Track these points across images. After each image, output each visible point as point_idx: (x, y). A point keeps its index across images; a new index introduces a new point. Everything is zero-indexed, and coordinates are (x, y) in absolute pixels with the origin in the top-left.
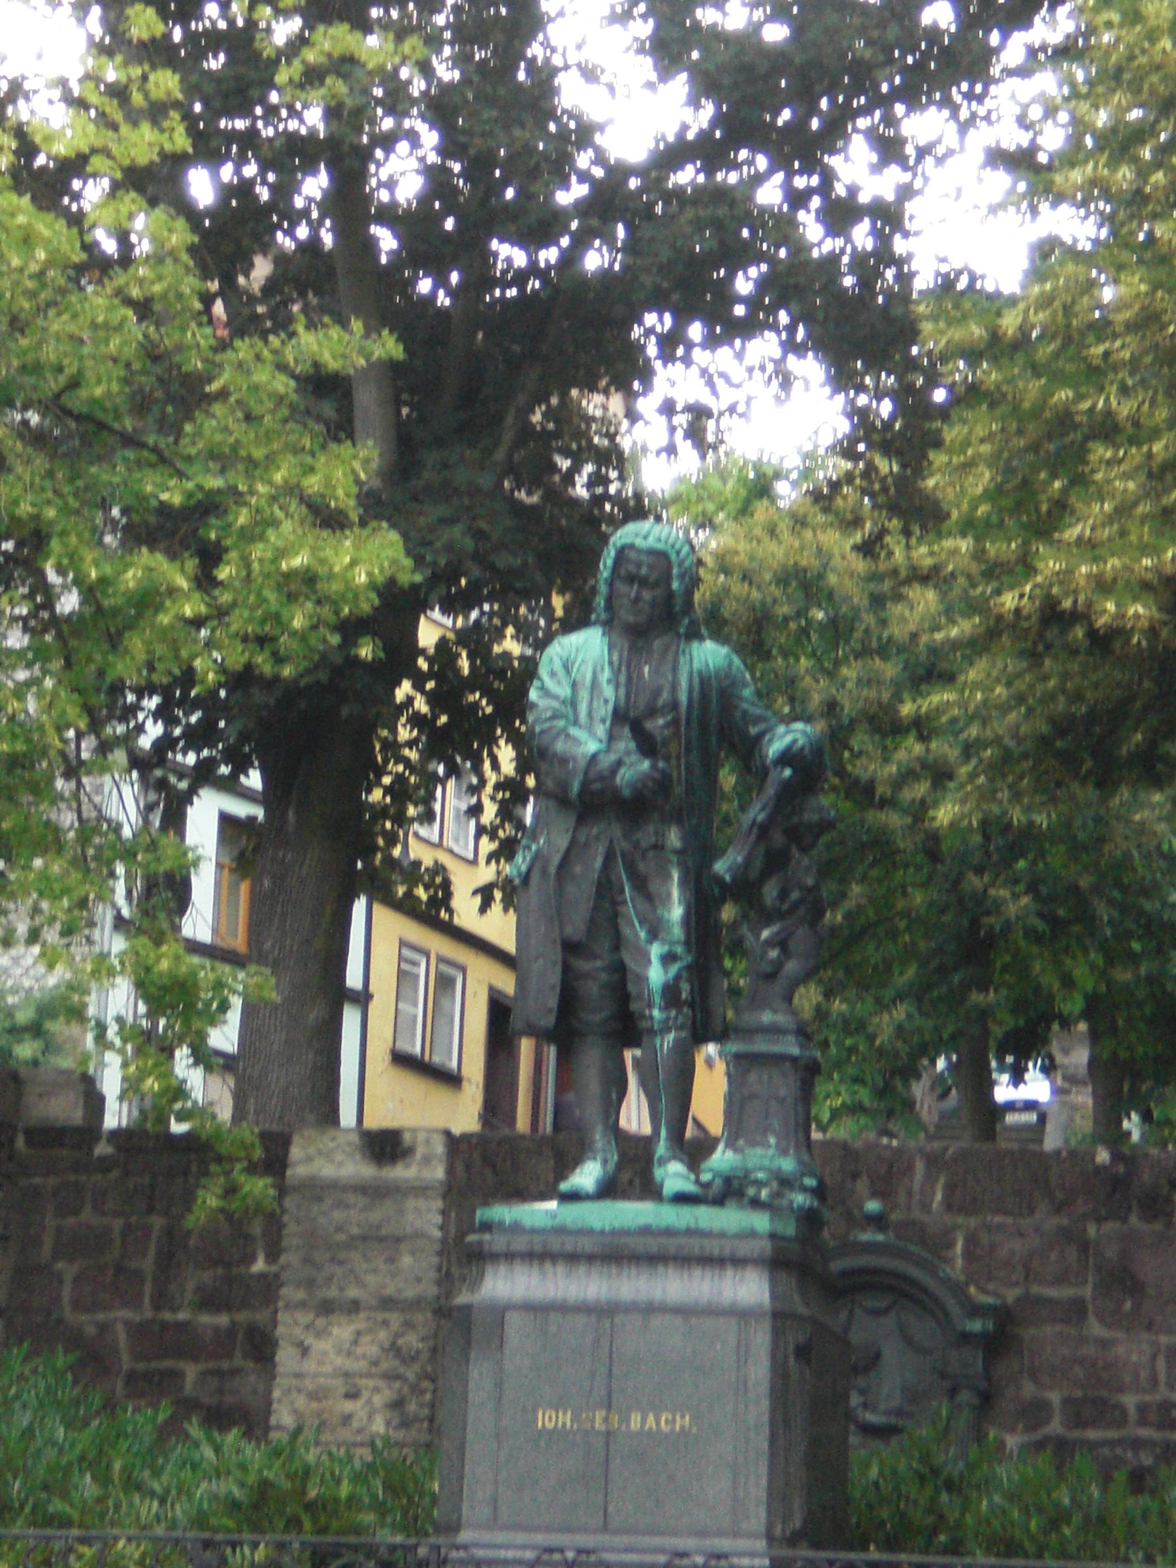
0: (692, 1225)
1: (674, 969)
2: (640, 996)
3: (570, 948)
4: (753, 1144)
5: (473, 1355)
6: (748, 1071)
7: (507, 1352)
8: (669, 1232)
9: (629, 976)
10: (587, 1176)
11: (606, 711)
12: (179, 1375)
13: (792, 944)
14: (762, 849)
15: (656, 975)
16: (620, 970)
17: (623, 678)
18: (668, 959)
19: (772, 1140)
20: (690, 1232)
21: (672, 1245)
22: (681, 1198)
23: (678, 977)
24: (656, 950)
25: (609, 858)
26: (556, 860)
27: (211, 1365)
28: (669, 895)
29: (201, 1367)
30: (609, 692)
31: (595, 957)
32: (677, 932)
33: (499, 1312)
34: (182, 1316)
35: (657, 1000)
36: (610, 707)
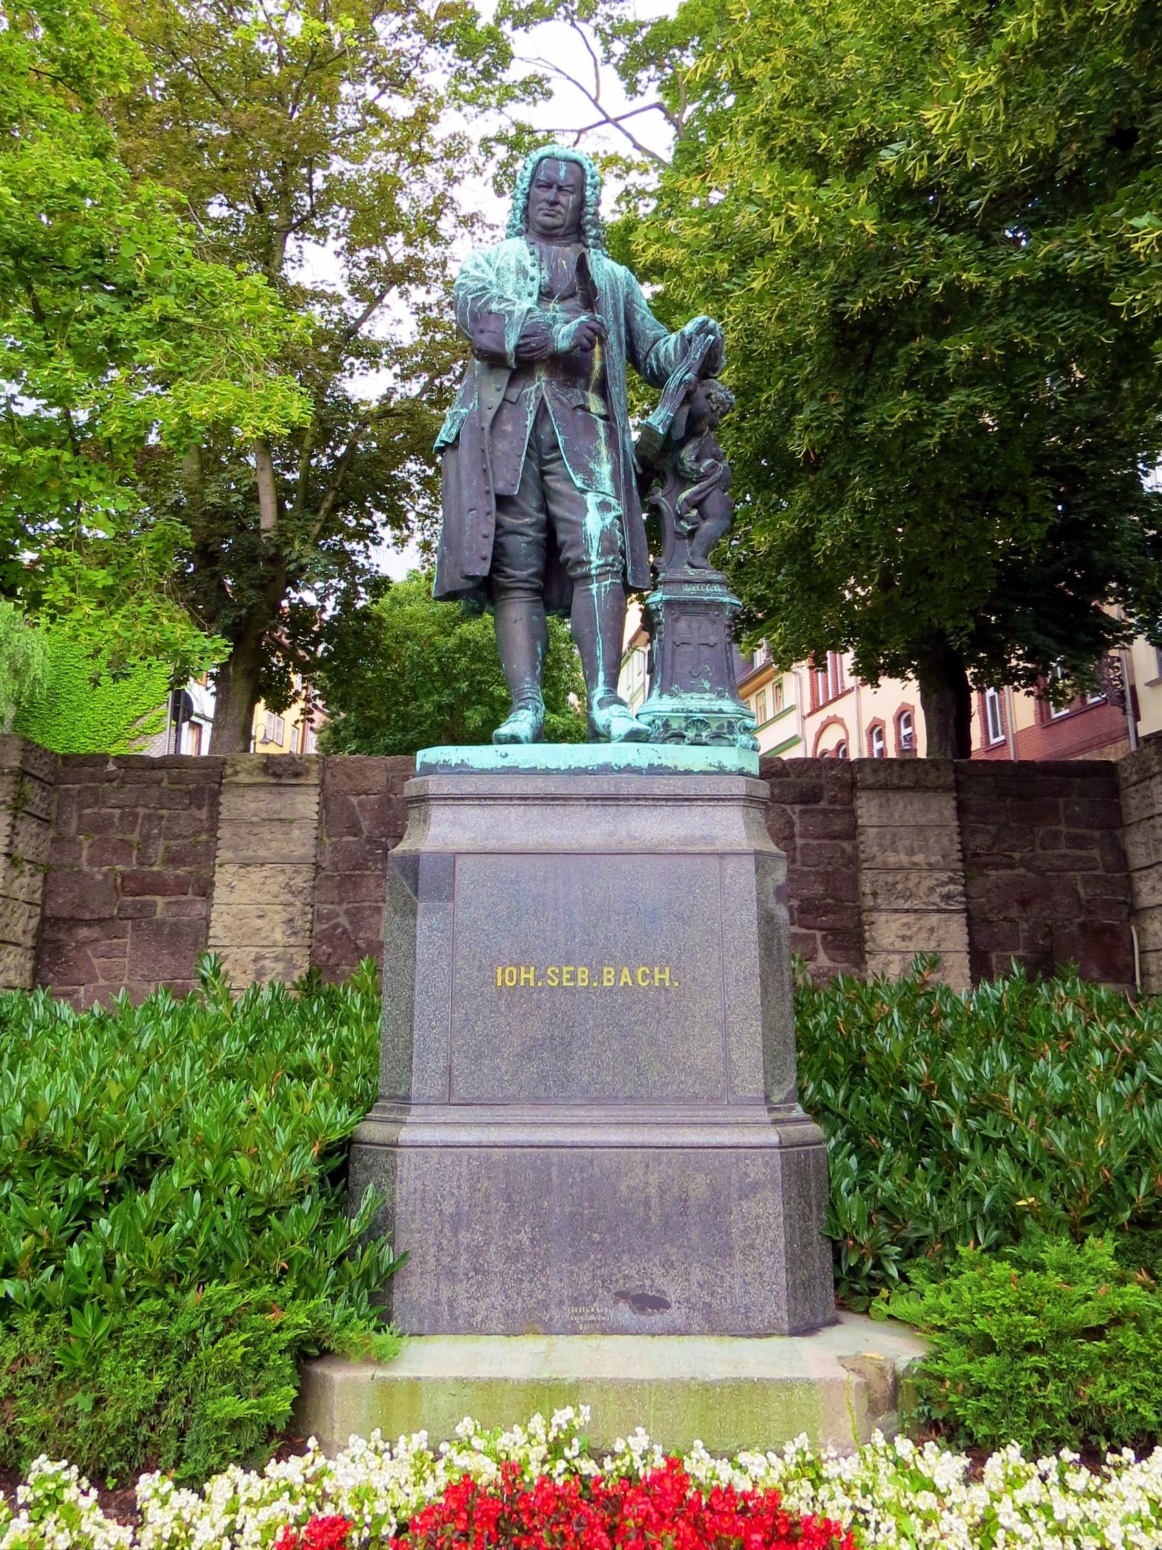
1: (610, 517)
2: (576, 544)
3: (503, 502)
4: (690, 689)
5: (421, 906)
6: (677, 620)
7: (458, 899)
8: (630, 769)
9: (560, 526)
10: (521, 722)
11: (534, 287)
12: (155, 904)
13: (709, 506)
14: (686, 409)
15: (594, 523)
16: (549, 526)
17: (544, 265)
18: (604, 507)
19: (707, 685)
20: (655, 770)
21: (631, 786)
22: (634, 736)
23: (612, 524)
24: (591, 499)
25: (542, 411)
26: (490, 414)
27: (172, 899)
29: (167, 899)
30: (533, 272)
31: (525, 514)
32: (607, 486)
33: (449, 860)
34: (155, 869)
35: (595, 544)
36: (536, 283)
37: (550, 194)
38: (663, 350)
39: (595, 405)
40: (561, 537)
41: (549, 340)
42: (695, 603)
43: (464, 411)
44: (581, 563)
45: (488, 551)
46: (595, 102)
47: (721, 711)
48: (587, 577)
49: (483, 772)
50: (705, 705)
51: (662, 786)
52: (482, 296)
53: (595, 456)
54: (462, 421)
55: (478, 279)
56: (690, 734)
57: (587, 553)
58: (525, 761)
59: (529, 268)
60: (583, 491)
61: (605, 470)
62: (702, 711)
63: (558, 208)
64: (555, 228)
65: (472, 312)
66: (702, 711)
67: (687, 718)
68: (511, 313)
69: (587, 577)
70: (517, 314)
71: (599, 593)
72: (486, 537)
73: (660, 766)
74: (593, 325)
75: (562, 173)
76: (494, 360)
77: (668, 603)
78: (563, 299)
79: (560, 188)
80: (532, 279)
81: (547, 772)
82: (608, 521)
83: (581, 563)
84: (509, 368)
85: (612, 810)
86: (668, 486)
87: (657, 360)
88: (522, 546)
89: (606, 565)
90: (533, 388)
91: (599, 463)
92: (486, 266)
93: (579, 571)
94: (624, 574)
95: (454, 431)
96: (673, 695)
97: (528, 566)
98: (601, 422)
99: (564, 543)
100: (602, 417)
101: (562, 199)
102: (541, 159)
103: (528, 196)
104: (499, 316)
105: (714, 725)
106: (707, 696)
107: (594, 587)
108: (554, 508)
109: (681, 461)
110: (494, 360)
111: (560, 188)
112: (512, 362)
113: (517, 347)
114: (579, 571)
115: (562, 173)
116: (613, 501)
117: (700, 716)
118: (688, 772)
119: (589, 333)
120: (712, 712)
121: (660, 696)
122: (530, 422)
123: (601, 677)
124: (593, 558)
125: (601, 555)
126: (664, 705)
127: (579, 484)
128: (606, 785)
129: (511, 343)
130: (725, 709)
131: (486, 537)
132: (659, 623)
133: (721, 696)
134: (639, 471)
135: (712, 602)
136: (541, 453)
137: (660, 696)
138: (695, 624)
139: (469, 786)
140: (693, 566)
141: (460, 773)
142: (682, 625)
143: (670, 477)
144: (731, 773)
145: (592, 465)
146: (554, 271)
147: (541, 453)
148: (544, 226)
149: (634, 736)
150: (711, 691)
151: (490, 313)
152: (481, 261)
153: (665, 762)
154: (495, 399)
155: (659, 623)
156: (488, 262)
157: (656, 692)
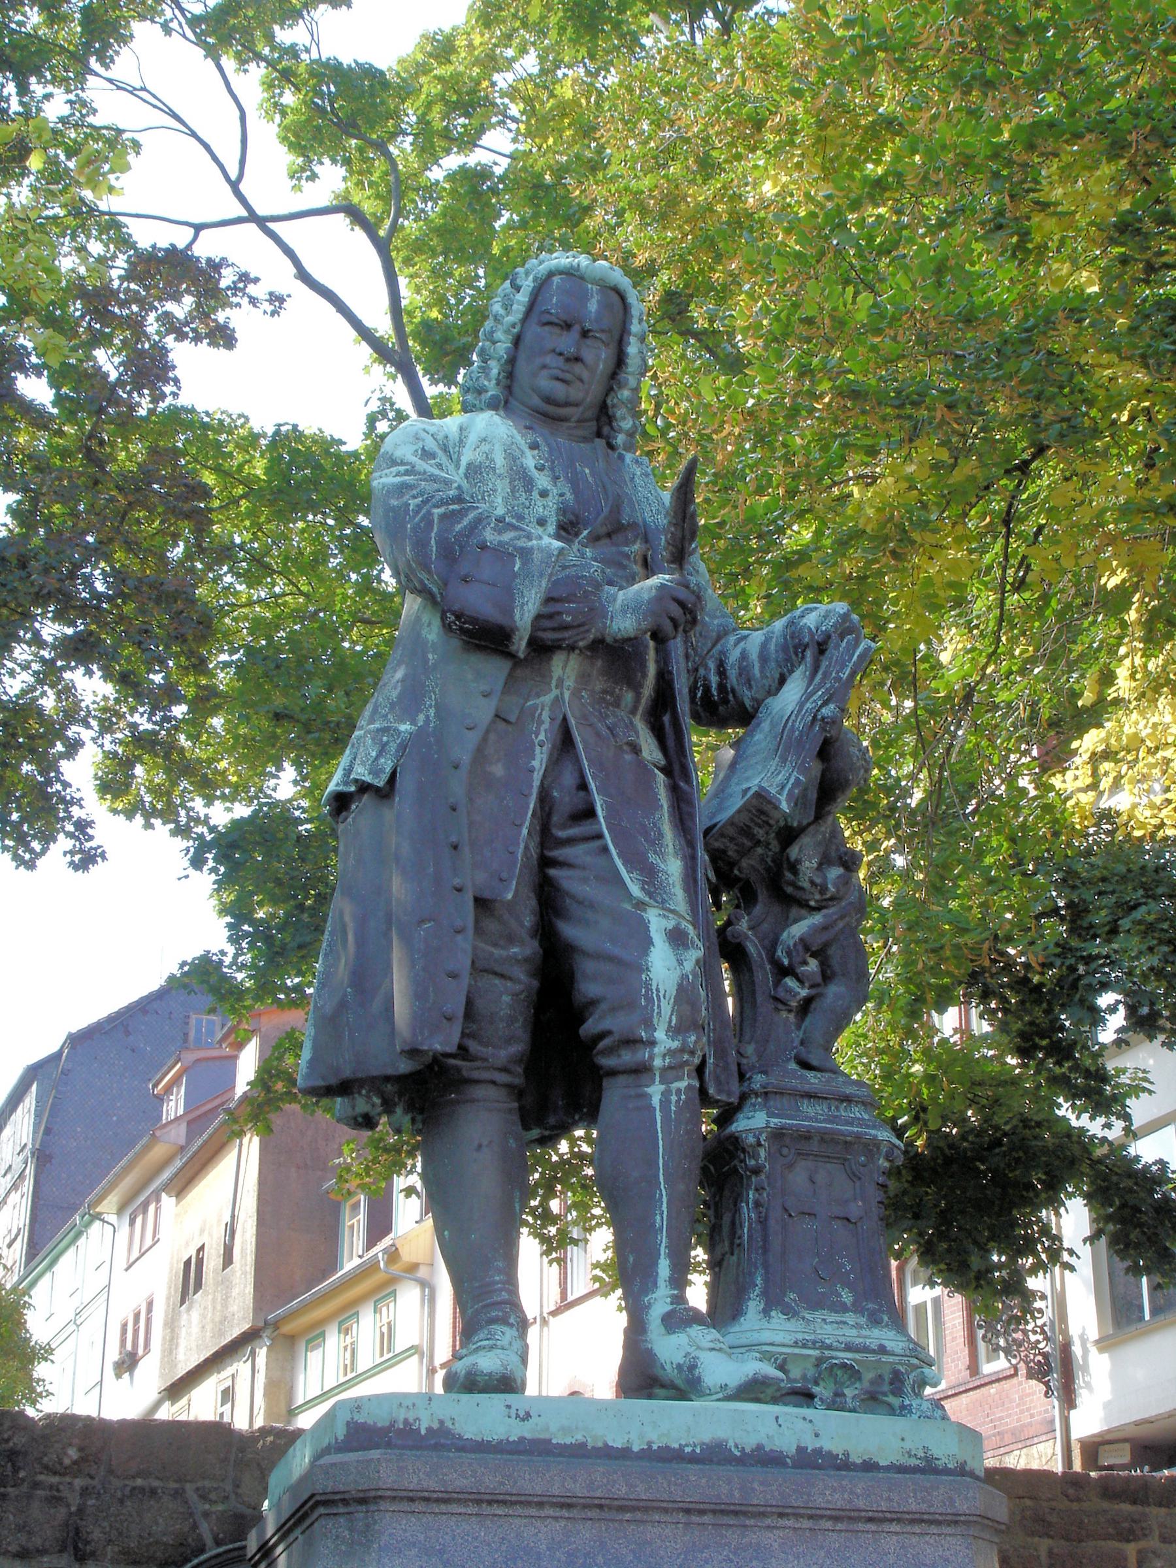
0: (811, 1444)
2: (630, 1004)
4: (816, 1304)
6: (791, 1166)
8: (765, 1459)
9: (586, 967)
11: (548, 508)
15: (665, 968)
18: (677, 938)
19: (847, 1297)
20: (810, 1461)
21: (764, 1489)
22: (753, 1390)
24: (657, 923)
28: (661, 835)
30: (542, 481)
31: (511, 939)
32: (679, 898)
35: (666, 1008)
36: (552, 502)
37: (567, 342)
38: (734, 656)
39: (650, 751)
40: (588, 988)
41: (597, 611)
42: (826, 1138)
43: (405, 727)
44: (631, 1042)
45: (457, 1005)
46: (235, 186)
47: (882, 1350)
48: (642, 1070)
49: (482, 1447)
50: (851, 1335)
51: (828, 1492)
52: (462, 513)
53: (656, 841)
54: (403, 747)
55: (433, 479)
56: (822, 1391)
57: (650, 1026)
58: (564, 1430)
59: (535, 474)
60: (641, 905)
61: (673, 867)
62: (849, 1348)
63: (578, 368)
64: (567, 404)
65: (443, 543)
66: (849, 1348)
67: (819, 1361)
68: (525, 553)
69: (642, 1070)
70: (537, 556)
71: (665, 1103)
72: (453, 976)
73: (818, 1452)
74: (683, 594)
75: (593, 306)
76: (485, 637)
77: (778, 1135)
78: (595, 539)
79: (585, 334)
80: (544, 494)
81: (608, 1453)
82: (689, 966)
83: (631, 1042)
84: (511, 656)
85: (732, 1536)
86: (758, 909)
87: (722, 672)
88: (508, 1000)
89: (682, 1050)
90: (547, 699)
91: (662, 855)
92: (442, 458)
93: (627, 1057)
94: (700, 1070)
95: (387, 765)
96: (789, 1312)
97: (509, 1040)
98: (661, 777)
99: (593, 1003)
100: (662, 770)
101: (588, 355)
102: (551, 274)
103: (517, 341)
104: (503, 554)
105: (868, 1376)
106: (851, 1318)
107: (655, 1091)
108: (569, 931)
109: (794, 868)
110: (485, 637)
111: (585, 334)
112: (520, 645)
113: (539, 617)
114: (627, 1057)
115: (593, 306)
116: (690, 930)
117: (847, 1357)
118: (869, 1466)
119: (676, 611)
120: (865, 1349)
121: (766, 1312)
122: (539, 761)
123: (664, 1268)
124: (660, 1035)
125: (675, 1031)
126: (769, 1330)
127: (635, 890)
128: (724, 1486)
129: (526, 609)
130: (889, 1345)
131: (453, 976)
132: (757, 1171)
133: (875, 1321)
134: (711, 875)
135: (858, 1136)
136: (561, 821)
137: (766, 1312)
138: (821, 1178)
139: (460, 1476)
140: (806, 1065)
141: (437, 1447)
142: (799, 1178)
143: (762, 895)
144: (946, 1471)
145: (652, 858)
146: (575, 483)
147: (561, 821)
148: (548, 400)
149: (753, 1390)
150: (857, 1308)
151: (483, 547)
152: (431, 445)
153: (831, 1444)
154: (483, 711)
155: (757, 1171)
156: (445, 449)
157: (754, 1306)
